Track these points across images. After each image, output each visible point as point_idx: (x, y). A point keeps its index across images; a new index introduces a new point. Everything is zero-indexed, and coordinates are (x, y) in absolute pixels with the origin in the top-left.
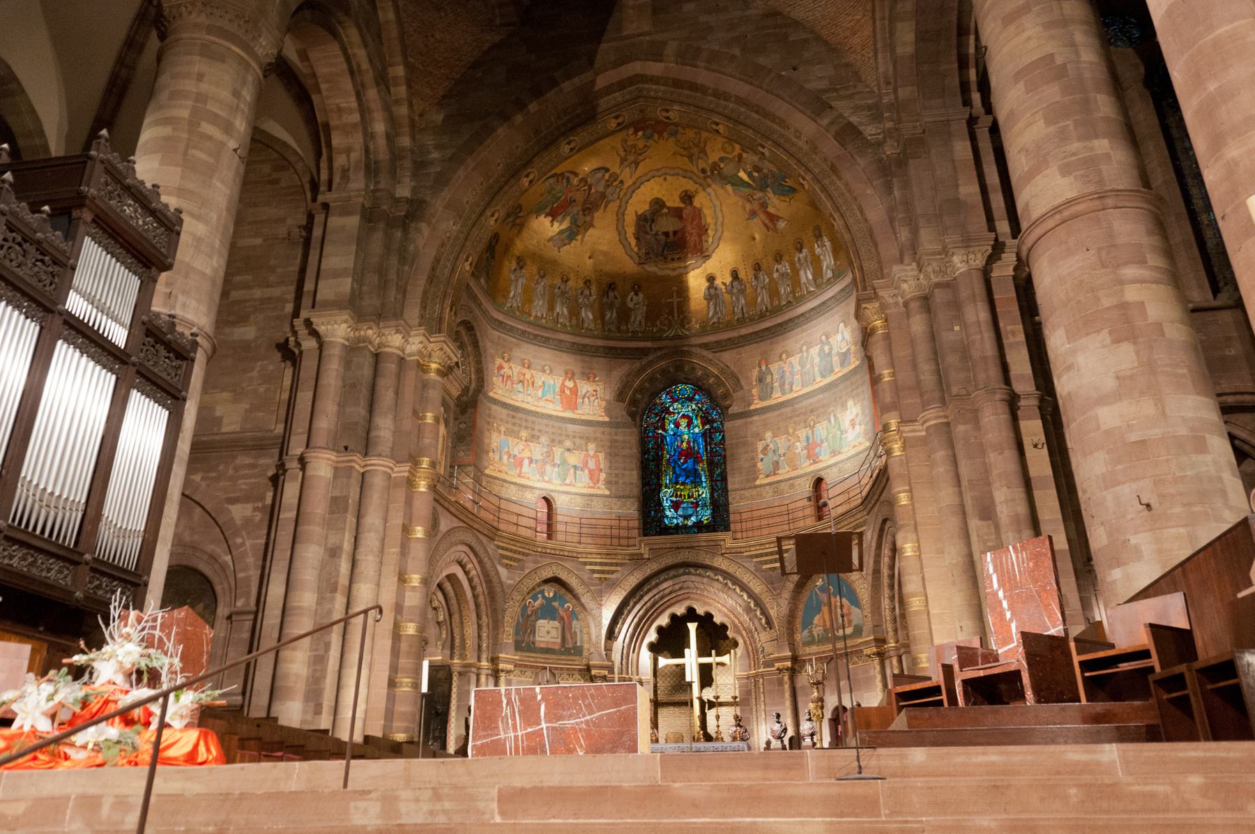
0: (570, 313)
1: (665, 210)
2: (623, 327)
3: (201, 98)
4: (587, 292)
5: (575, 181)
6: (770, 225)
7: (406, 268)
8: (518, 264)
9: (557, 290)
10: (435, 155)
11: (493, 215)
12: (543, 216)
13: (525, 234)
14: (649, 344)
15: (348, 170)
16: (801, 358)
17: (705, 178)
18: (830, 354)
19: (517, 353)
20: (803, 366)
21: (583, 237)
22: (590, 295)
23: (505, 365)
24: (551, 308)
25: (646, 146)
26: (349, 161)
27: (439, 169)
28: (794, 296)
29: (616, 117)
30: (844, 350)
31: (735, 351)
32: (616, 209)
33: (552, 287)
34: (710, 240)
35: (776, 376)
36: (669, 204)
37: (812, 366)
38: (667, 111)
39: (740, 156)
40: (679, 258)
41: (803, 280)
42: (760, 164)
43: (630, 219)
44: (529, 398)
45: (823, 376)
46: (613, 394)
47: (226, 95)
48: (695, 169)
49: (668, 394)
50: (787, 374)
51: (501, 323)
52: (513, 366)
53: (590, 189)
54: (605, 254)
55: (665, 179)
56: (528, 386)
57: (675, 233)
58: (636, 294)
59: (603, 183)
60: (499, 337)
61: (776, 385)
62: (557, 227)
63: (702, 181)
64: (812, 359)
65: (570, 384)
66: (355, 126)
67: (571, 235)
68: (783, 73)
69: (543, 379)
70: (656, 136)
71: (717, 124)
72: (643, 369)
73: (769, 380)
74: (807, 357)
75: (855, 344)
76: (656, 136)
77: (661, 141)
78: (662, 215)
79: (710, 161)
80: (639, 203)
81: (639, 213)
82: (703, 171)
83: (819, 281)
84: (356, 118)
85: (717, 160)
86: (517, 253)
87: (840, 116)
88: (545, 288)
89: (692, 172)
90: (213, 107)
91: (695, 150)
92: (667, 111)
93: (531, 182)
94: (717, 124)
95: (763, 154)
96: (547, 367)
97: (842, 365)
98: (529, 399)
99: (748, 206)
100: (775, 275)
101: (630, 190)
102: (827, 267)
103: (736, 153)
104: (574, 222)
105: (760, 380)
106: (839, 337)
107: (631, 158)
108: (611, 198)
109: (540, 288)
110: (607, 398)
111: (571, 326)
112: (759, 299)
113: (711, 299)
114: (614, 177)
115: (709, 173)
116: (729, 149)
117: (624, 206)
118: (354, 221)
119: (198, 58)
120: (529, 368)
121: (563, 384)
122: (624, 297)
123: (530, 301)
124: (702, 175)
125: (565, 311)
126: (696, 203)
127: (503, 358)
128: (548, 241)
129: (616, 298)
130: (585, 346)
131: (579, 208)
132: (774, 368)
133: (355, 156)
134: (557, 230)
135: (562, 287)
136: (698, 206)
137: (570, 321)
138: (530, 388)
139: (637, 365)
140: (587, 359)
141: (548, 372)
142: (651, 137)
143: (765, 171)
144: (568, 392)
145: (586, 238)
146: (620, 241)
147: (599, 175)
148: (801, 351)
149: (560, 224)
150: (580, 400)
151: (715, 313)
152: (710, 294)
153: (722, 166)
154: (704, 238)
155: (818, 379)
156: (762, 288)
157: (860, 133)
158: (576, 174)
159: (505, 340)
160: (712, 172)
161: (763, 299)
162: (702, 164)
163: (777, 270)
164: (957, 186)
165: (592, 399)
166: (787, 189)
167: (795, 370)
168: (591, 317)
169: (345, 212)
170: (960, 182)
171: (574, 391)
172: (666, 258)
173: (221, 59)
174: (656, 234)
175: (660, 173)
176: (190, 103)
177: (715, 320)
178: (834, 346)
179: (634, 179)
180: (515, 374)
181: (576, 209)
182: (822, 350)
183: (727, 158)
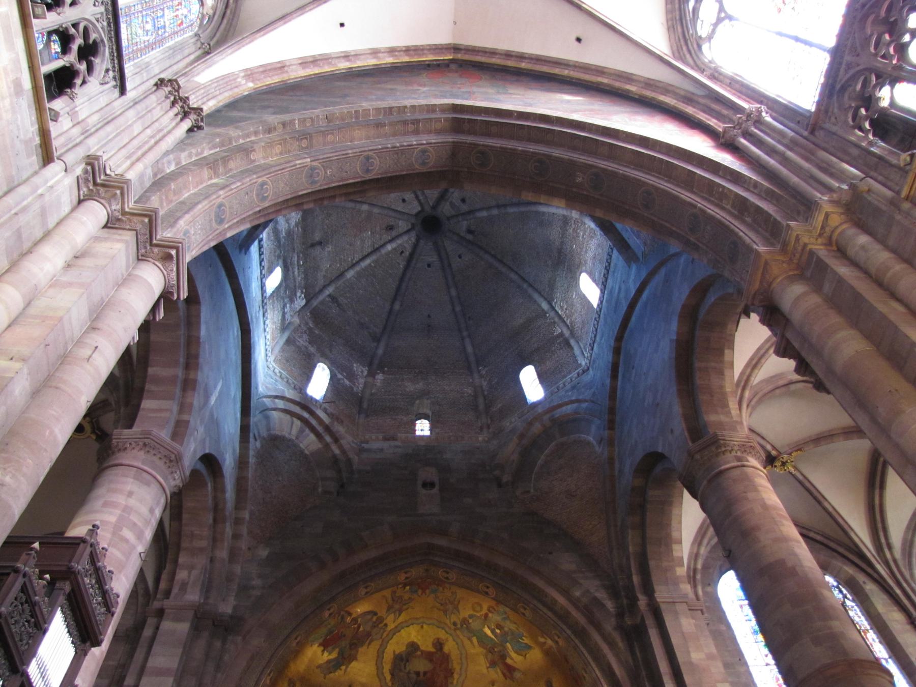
1: (419, 653)
3: (127, 509)
5: (348, 620)
6: (508, 674)
7: (219, 675)
10: (257, 582)
11: (296, 639)
15: (187, 583)
17: (455, 630)
21: (346, 668)
25: (410, 598)
26: (189, 577)
27: (259, 594)
29: (406, 573)
32: (378, 647)
34: (455, 682)
36: (423, 648)
39: (486, 616)
42: (502, 624)
43: (388, 656)
47: (144, 510)
48: (448, 622)
53: (359, 627)
57: (425, 673)
59: (370, 624)
62: (326, 657)
63: (453, 632)
66: (202, 550)
67: (335, 665)
68: (542, 555)
70: (420, 592)
71: (488, 587)
79: (461, 617)
80: (396, 646)
81: (397, 653)
82: (455, 624)
84: (203, 543)
85: (467, 616)
87: (588, 591)
89: (445, 624)
90: (134, 518)
91: (450, 607)
92: (448, 573)
94: (488, 587)
95: (524, 614)
99: (490, 655)
103: (483, 612)
104: (341, 654)
107: (397, 606)
115: (459, 626)
116: (478, 608)
118: (183, 627)
119: (132, 480)
124: (453, 627)
126: (446, 649)
133: (195, 573)
142: (416, 591)
143: (506, 629)
145: (349, 669)
147: (369, 617)
153: (470, 621)
154: (450, 680)
158: (350, 614)
160: (462, 626)
164: (688, 653)
166: (523, 645)
169: (177, 619)
170: (690, 649)
173: (148, 484)
174: (409, 673)
176: (118, 512)
179: (396, 624)
181: (344, 643)
183: (475, 616)
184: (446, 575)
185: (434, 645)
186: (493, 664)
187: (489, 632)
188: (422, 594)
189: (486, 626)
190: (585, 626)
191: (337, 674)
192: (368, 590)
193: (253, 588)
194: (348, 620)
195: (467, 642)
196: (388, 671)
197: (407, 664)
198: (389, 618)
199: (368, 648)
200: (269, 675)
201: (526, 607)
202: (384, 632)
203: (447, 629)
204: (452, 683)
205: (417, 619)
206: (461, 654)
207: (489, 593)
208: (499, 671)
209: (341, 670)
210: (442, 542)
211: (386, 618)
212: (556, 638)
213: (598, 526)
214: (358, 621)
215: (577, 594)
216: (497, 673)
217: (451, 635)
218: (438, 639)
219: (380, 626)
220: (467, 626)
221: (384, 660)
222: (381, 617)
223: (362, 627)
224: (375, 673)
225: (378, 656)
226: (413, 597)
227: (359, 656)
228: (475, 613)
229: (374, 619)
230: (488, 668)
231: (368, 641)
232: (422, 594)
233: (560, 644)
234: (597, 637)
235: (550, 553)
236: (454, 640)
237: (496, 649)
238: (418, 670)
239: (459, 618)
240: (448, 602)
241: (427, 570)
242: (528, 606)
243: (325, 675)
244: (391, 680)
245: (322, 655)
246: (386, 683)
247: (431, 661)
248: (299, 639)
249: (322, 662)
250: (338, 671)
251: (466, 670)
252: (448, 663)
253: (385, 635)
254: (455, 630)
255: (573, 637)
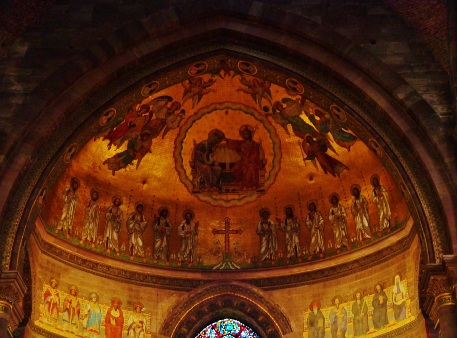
0: (119, 237)
1: (224, 142)
2: (173, 256)
4: (139, 218)
8: (72, 185)
9: (108, 214)
10: (17, 87)
11: (70, 151)
12: (101, 138)
13: (82, 157)
14: (198, 276)
16: (355, 304)
18: (384, 305)
19: (64, 279)
20: (356, 314)
22: (142, 221)
23: (53, 292)
24: (102, 232)
28: (349, 242)
29: (197, 66)
30: (399, 303)
31: (286, 290)
32: (174, 137)
33: (104, 210)
34: (267, 175)
35: (328, 321)
36: (227, 137)
37: (366, 315)
38: (248, 65)
40: (234, 191)
41: (359, 226)
44: (74, 327)
45: (377, 327)
46: (159, 327)
48: (257, 106)
49: (212, 329)
50: (340, 320)
51: (51, 246)
52: (60, 292)
53: (151, 115)
54: (159, 179)
55: (227, 113)
56: (74, 314)
57: (232, 165)
58: (188, 223)
59: (164, 110)
60: (48, 262)
61: (328, 330)
64: (366, 307)
65: (115, 314)
69: (89, 307)
70: (222, 73)
72: (191, 301)
73: (320, 324)
74: (361, 305)
75: (412, 298)
76: (222, 73)
77: (227, 78)
78: (221, 147)
79: (273, 102)
82: (266, 109)
83: (376, 229)
86: (72, 174)
87: (415, 93)
88: (96, 211)
89: (256, 109)
92: (248, 65)
93: (109, 120)
94: (295, 83)
95: (338, 116)
96: (93, 295)
97: (397, 317)
98: (74, 329)
100: (331, 217)
101: (191, 120)
102: (384, 217)
105: (312, 323)
106: (395, 289)
107: (196, 90)
108: (171, 126)
109: (92, 211)
110: (153, 330)
111: (120, 252)
112: (313, 240)
113: (264, 235)
114: (177, 106)
115: (271, 112)
117: (182, 133)
120: (75, 295)
121: (109, 313)
122: (177, 224)
123: (82, 225)
124: (263, 112)
125: (115, 235)
126: (256, 138)
127: (51, 284)
128: (104, 163)
129: (167, 225)
130: (133, 273)
131: (138, 133)
132: (327, 312)
134: (114, 153)
135: (114, 211)
136: (257, 141)
137: (120, 247)
138: (76, 317)
139: (186, 295)
140: (134, 287)
141: (94, 300)
144: (113, 322)
145: (142, 163)
146: (176, 168)
147: (162, 103)
148: (355, 298)
149: (118, 148)
150: (125, 332)
151: (268, 249)
152: (263, 229)
153: (285, 106)
154: (260, 172)
155: (372, 329)
156: (316, 229)
157: (433, 111)
159: (53, 265)
160: (274, 111)
161: (317, 240)
162: (265, 103)
163: (333, 213)
165: (138, 330)
167: (348, 317)
168: (141, 243)
171: (120, 321)
172: (220, 189)
174: (213, 164)
175: (222, 107)
177: (267, 256)
178: (389, 297)
179: (195, 110)
180: (62, 301)
181: (134, 134)
182: (376, 300)
184: (245, 68)
185: (241, 132)
186: (311, 156)
187: (306, 120)
188: (225, 75)
189: (303, 112)
190: (407, 135)
191: (128, 169)
192: (152, 88)
193: (14, 95)
194: (138, 107)
195: (280, 130)
196: (188, 164)
197: (211, 155)
198: (186, 104)
199: (163, 138)
200: (41, 194)
201: (340, 108)
202: (181, 120)
203: (256, 114)
204: (264, 176)
205: (221, 103)
206: (274, 143)
207: (297, 89)
208: (318, 163)
209: (132, 164)
210: (241, 28)
211: (183, 104)
212: (374, 146)
213: (438, 6)
214: (149, 108)
215: (401, 96)
216: (316, 166)
217: (261, 121)
218: (246, 126)
219: (176, 113)
220: (281, 112)
221: (182, 152)
222: (177, 102)
223: (154, 115)
224: (173, 166)
225: (175, 148)
226: (214, 79)
227: (152, 148)
228: (290, 97)
229: (169, 105)
230: (304, 160)
231: (163, 131)
232: (225, 75)
233: (378, 152)
234: (420, 150)
235: (373, 42)
236: (265, 127)
237: (314, 139)
238: (223, 162)
239: (271, 103)
240: (256, 83)
241: (222, 62)
242: (343, 109)
243: (114, 171)
244: (192, 174)
245: (109, 149)
246: (187, 177)
247: (238, 150)
248: (73, 151)
249: (110, 157)
250: (130, 165)
251: (280, 162)
252: (259, 153)
253: (182, 122)
254: (267, 116)
255: (392, 147)
